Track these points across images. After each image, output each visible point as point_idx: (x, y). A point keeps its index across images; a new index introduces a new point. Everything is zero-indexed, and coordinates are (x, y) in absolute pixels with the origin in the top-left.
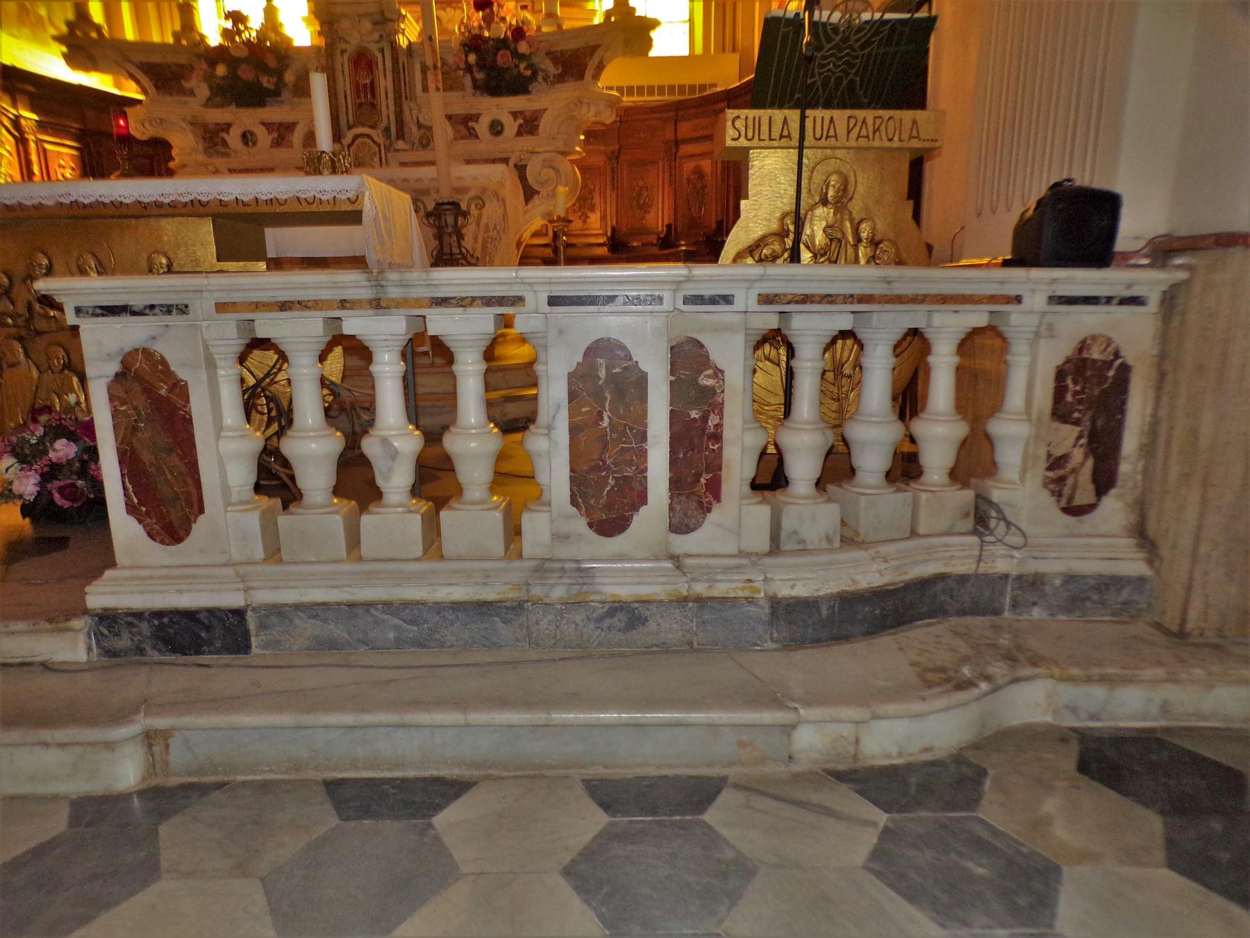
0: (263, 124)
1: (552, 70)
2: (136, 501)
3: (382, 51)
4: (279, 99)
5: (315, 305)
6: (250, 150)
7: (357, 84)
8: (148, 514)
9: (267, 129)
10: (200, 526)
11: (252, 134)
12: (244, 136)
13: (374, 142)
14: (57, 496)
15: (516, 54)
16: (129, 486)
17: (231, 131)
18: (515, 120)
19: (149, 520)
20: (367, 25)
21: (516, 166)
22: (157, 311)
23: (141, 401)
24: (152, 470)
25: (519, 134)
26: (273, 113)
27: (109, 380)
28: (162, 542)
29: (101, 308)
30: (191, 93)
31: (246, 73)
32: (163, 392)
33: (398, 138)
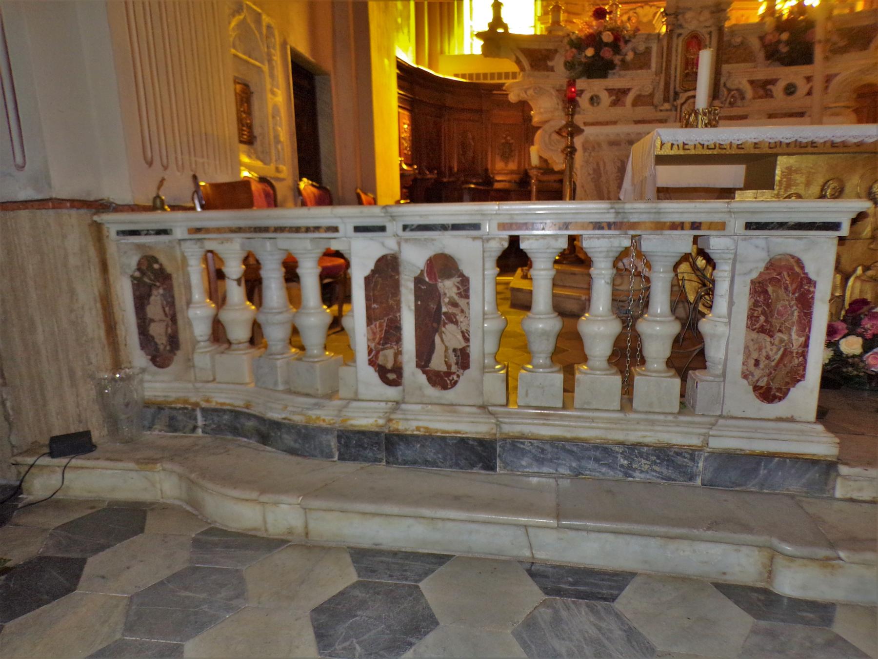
0: (607, 90)
3: (710, 33)
7: (687, 59)
9: (609, 93)
11: (597, 97)
12: (592, 99)
17: (583, 95)
20: (706, 14)
26: (615, 81)
30: (552, 69)
31: (607, 53)
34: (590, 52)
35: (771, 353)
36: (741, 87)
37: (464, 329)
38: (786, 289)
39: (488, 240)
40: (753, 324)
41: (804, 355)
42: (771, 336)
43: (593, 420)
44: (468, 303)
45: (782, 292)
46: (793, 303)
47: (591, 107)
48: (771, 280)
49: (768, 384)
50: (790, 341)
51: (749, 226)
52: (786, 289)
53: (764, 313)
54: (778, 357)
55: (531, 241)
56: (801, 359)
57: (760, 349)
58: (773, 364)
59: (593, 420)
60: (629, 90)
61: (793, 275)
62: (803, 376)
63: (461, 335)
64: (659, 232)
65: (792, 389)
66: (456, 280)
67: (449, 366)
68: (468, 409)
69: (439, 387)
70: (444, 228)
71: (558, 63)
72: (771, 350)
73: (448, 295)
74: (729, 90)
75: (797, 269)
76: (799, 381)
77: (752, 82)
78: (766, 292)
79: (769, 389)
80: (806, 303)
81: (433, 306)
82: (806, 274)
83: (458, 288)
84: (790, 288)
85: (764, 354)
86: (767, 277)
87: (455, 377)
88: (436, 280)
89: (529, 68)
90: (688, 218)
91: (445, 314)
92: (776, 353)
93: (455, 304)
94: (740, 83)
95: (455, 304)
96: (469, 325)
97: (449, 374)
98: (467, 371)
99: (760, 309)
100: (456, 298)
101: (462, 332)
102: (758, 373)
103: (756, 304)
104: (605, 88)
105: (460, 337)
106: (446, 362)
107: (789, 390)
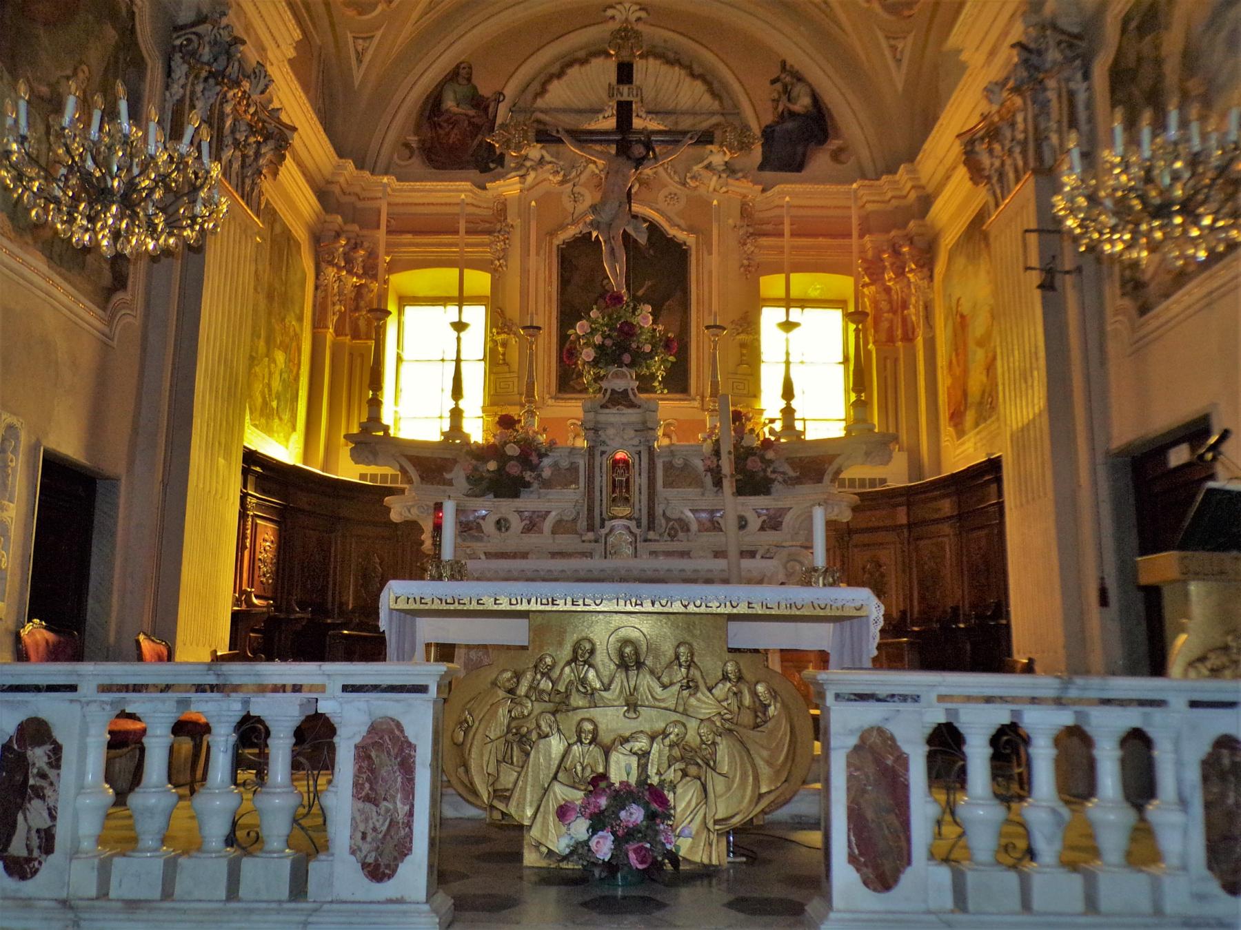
1: (791, 473)
2: (856, 852)
3: (639, 453)
5: (1003, 700)
7: (614, 481)
8: (865, 864)
10: (908, 878)
11: (506, 520)
12: (498, 522)
13: (631, 532)
14: (632, 856)
15: (762, 459)
16: (853, 838)
19: (865, 870)
22: (896, 699)
23: (871, 769)
24: (873, 826)
25: (762, 529)
26: (528, 502)
27: (848, 750)
28: (875, 890)
29: (855, 695)
30: (450, 483)
31: (514, 469)
32: (889, 762)
33: (649, 529)
34: (492, 466)
35: (378, 825)
37: (51, 805)
38: (389, 753)
39: (88, 703)
40: (358, 792)
41: (409, 825)
42: (377, 806)
43: (185, 911)
44: (58, 775)
45: (384, 756)
46: (395, 768)
47: (497, 532)
48: (374, 744)
49: (376, 860)
50: (396, 810)
51: (345, 688)
52: (389, 753)
53: (368, 780)
54: (384, 828)
55: (137, 705)
56: (407, 829)
57: (367, 820)
58: (380, 836)
59: (185, 911)
61: (394, 739)
62: (410, 849)
63: (47, 811)
64: (261, 694)
65: (400, 865)
66: (48, 747)
67: (30, 850)
68: (46, 903)
69: (17, 878)
70: (37, 689)
71: (458, 475)
72: (378, 821)
73: (37, 765)
74: (668, 519)
75: (397, 732)
76: (406, 855)
78: (369, 757)
79: (377, 866)
80: (407, 768)
81: (19, 778)
82: (406, 737)
83: (49, 757)
84: (392, 753)
85: (371, 825)
86: (370, 741)
87: (36, 864)
88: (26, 748)
89: (419, 479)
90: (289, 681)
91: (32, 787)
92: (382, 825)
93: (43, 776)
94: (682, 512)
95: (43, 776)
96: (57, 800)
97: (29, 860)
98: (51, 857)
99: (364, 776)
100: (46, 768)
101: (49, 809)
102: (366, 847)
103: (360, 769)
105: (45, 814)
106: (27, 846)
107: (397, 866)
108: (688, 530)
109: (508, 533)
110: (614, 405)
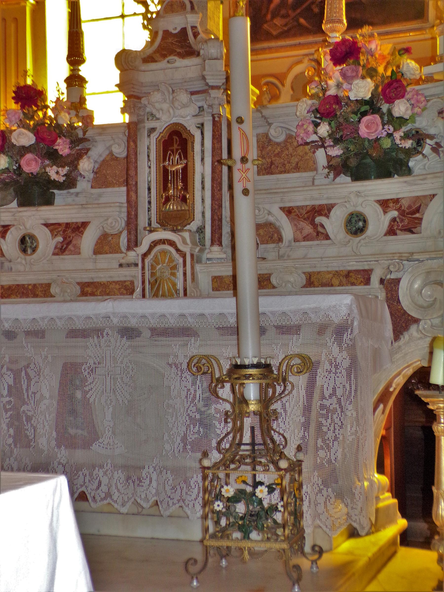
0: (47, 225)
3: (201, 127)
4: (72, 191)
6: (28, 258)
7: (165, 171)
9: (51, 231)
11: (32, 237)
12: (23, 240)
13: (178, 250)
18: (385, 212)
21: (382, 281)
25: (391, 232)
36: (271, 219)
47: (22, 255)
60: (85, 225)
77: (288, 211)
94: (270, 213)
104: (43, 222)
108: (280, 240)
109: (35, 256)
110: (164, 56)
